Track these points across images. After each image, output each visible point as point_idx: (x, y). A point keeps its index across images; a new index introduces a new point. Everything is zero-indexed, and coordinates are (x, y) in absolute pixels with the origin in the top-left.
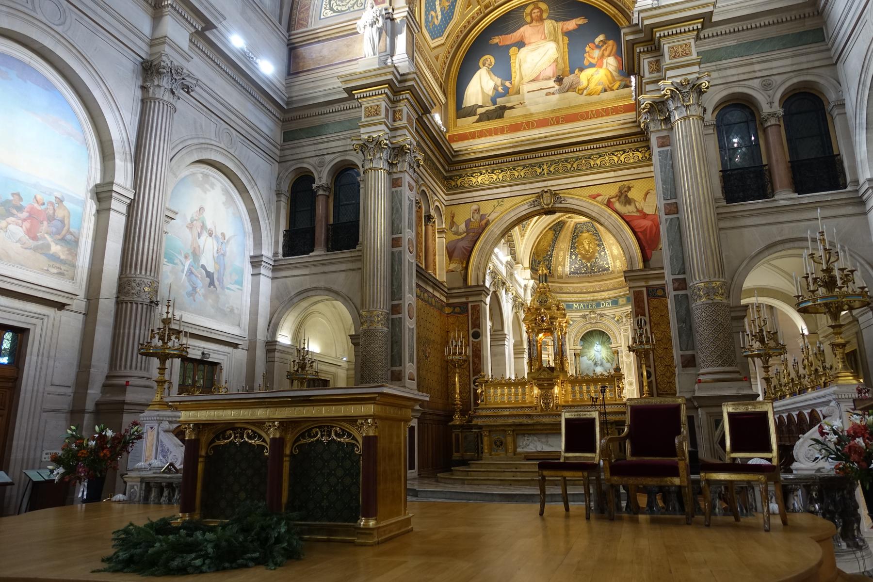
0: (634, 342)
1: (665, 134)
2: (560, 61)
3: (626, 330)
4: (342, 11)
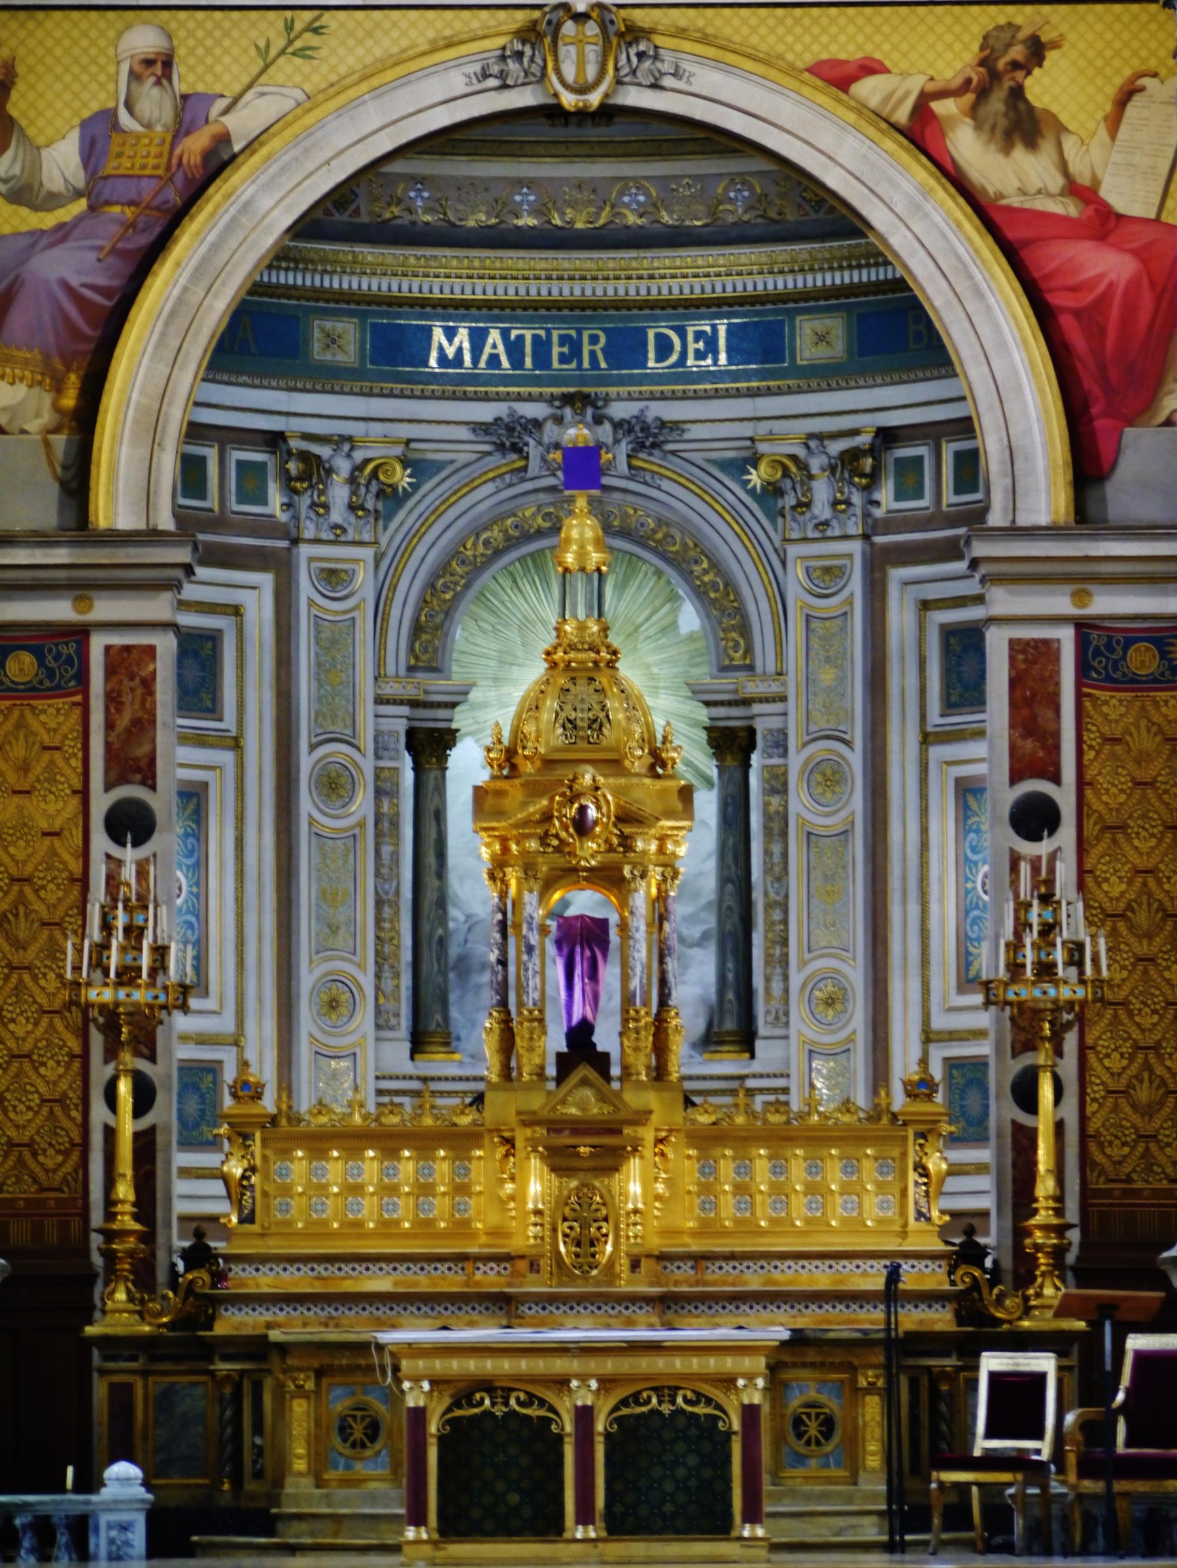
0: (1016, 969)
3: (828, 575)
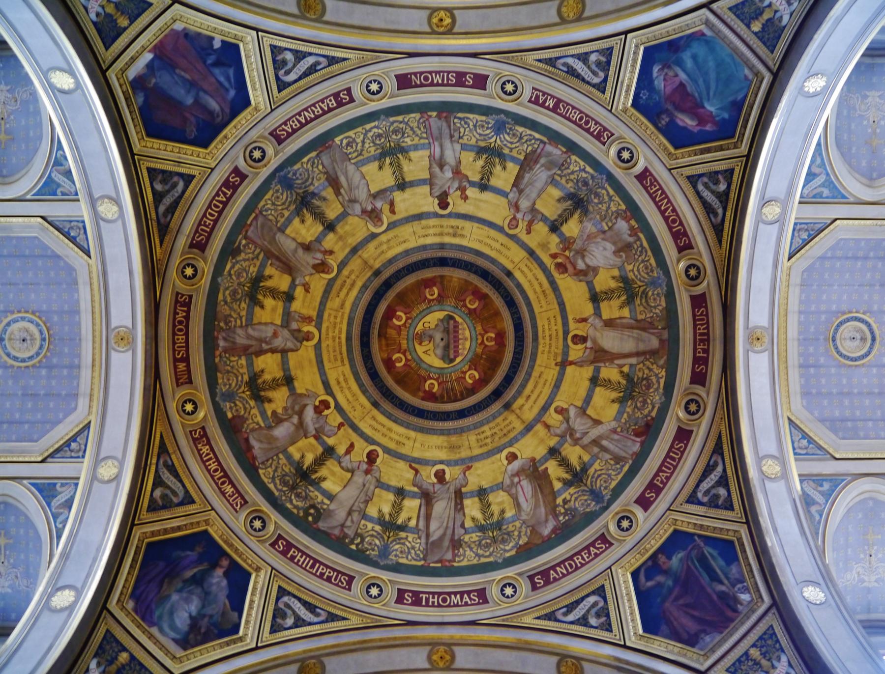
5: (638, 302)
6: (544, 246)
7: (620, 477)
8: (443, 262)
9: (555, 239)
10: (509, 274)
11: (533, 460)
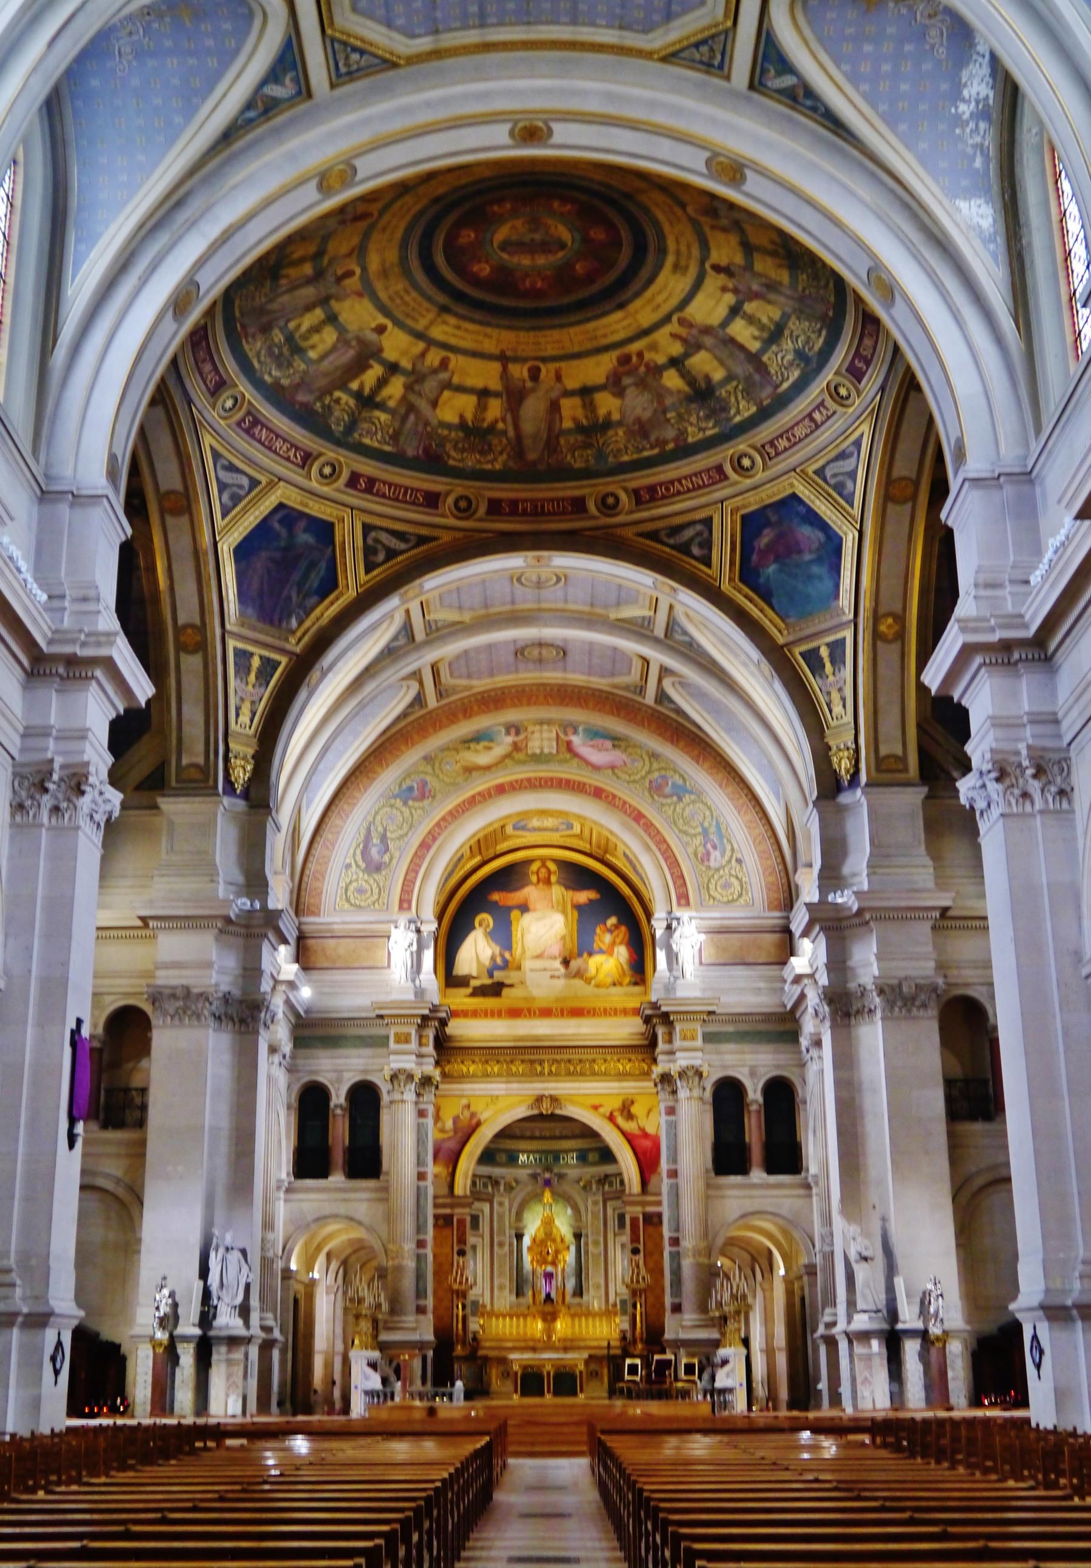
1: (671, 1104)
2: (568, 939)
3: (595, 1203)
4: (360, 907)
5: (580, 438)
6: (653, 347)
7: (376, 445)
8: (640, 250)
9: (661, 359)
10: (621, 306)
11: (381, 350)
